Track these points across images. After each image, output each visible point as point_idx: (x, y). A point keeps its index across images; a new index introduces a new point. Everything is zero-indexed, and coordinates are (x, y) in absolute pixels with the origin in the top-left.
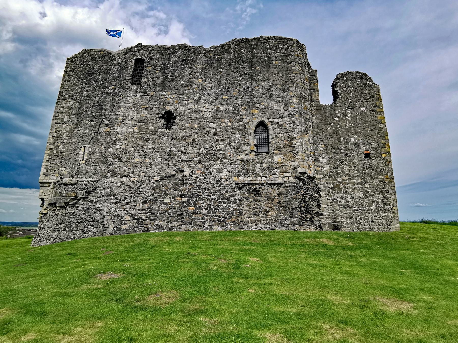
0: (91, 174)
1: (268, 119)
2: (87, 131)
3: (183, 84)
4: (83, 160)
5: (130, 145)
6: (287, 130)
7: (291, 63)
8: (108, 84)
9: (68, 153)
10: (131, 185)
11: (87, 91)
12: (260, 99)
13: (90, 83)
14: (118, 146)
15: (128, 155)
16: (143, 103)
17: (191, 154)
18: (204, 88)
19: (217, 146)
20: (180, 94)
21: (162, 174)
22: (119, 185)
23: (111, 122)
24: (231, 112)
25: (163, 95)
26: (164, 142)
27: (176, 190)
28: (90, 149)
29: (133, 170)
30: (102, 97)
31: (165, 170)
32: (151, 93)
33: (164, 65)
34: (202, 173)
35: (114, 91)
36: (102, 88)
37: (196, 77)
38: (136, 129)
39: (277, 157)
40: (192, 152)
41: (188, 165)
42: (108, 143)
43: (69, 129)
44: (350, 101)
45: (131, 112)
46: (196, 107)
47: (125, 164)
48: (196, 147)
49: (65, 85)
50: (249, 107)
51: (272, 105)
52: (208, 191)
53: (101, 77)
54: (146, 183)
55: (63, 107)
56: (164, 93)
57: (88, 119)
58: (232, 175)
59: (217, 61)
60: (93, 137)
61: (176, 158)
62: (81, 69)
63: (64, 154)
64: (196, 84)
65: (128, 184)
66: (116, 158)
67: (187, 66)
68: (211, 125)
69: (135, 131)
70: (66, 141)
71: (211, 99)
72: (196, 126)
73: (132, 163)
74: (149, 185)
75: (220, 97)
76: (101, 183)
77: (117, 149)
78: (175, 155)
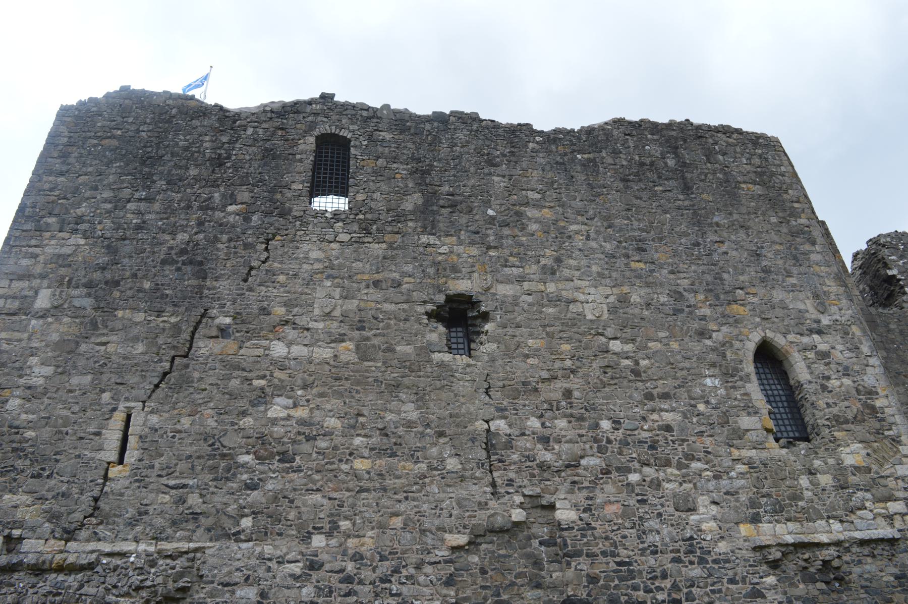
0: (159, 522)
1: (785, 335)
2: (140, 348)
3: (493, 218)
4: (121, 461)
5: (328, 407)
6: (846, 368)
7: (786, 192)
8: (223, 196)
9: (47, 433)
10: (350, 567)
11: (139, 213)
12: (741, 278)
13: (149, 188)
14: (277, 409)
15: (323, 444)
16: (360, 265)
17: (570, 441)
18: (563, 235)
19: (655, 416)
20: (489, 248)
21: (474, 521)
22: (296, 569)
23: (243, 322)
24: (667, 309)
25: (428, 245)
26: (462, 400)
27: (538, 586)
28: (154, 419)
29: (353, 506)
30: (201, 236)
31: (483, 505)
32: (388, 238)
33: (419, 160)
34: (627, 512)
35: (247, 219)
36: (200, 208)
37: (532, 203)
38: (347, 351)
39: (848, 450)
40: (571, 434)
41: (567, 485)
42: (233, 396)
43: (55, 337)
45: (320, 293)
46: (551, 287)
47: (314, 482)
48: (581, 419)
49: (47, 186)
50: (717, 297)
51: (778, 295)
52: (667, 584)
53: (193, 172)
54: (413, 558)
55: (35, 256)
56: (432, 240)
57: (143, 305)
58: (733, 515)
59: (584, 165)
60: (165, 374)
61: (515, 457)
62: (115, 143)
63: (30, 434)
64: (538, 221)
65: (337, 565)
66: (271, 456)
67: (498, 170)
68: (615, 346)
69: (343, 358)
70: (41, 381)
71: (595, 268)
72: (566, 347)
73: (342, 477)
74: (428, 569)
75: (620, 263)
76: (211, 561)
77: (274, 421)
78: (509, 445)
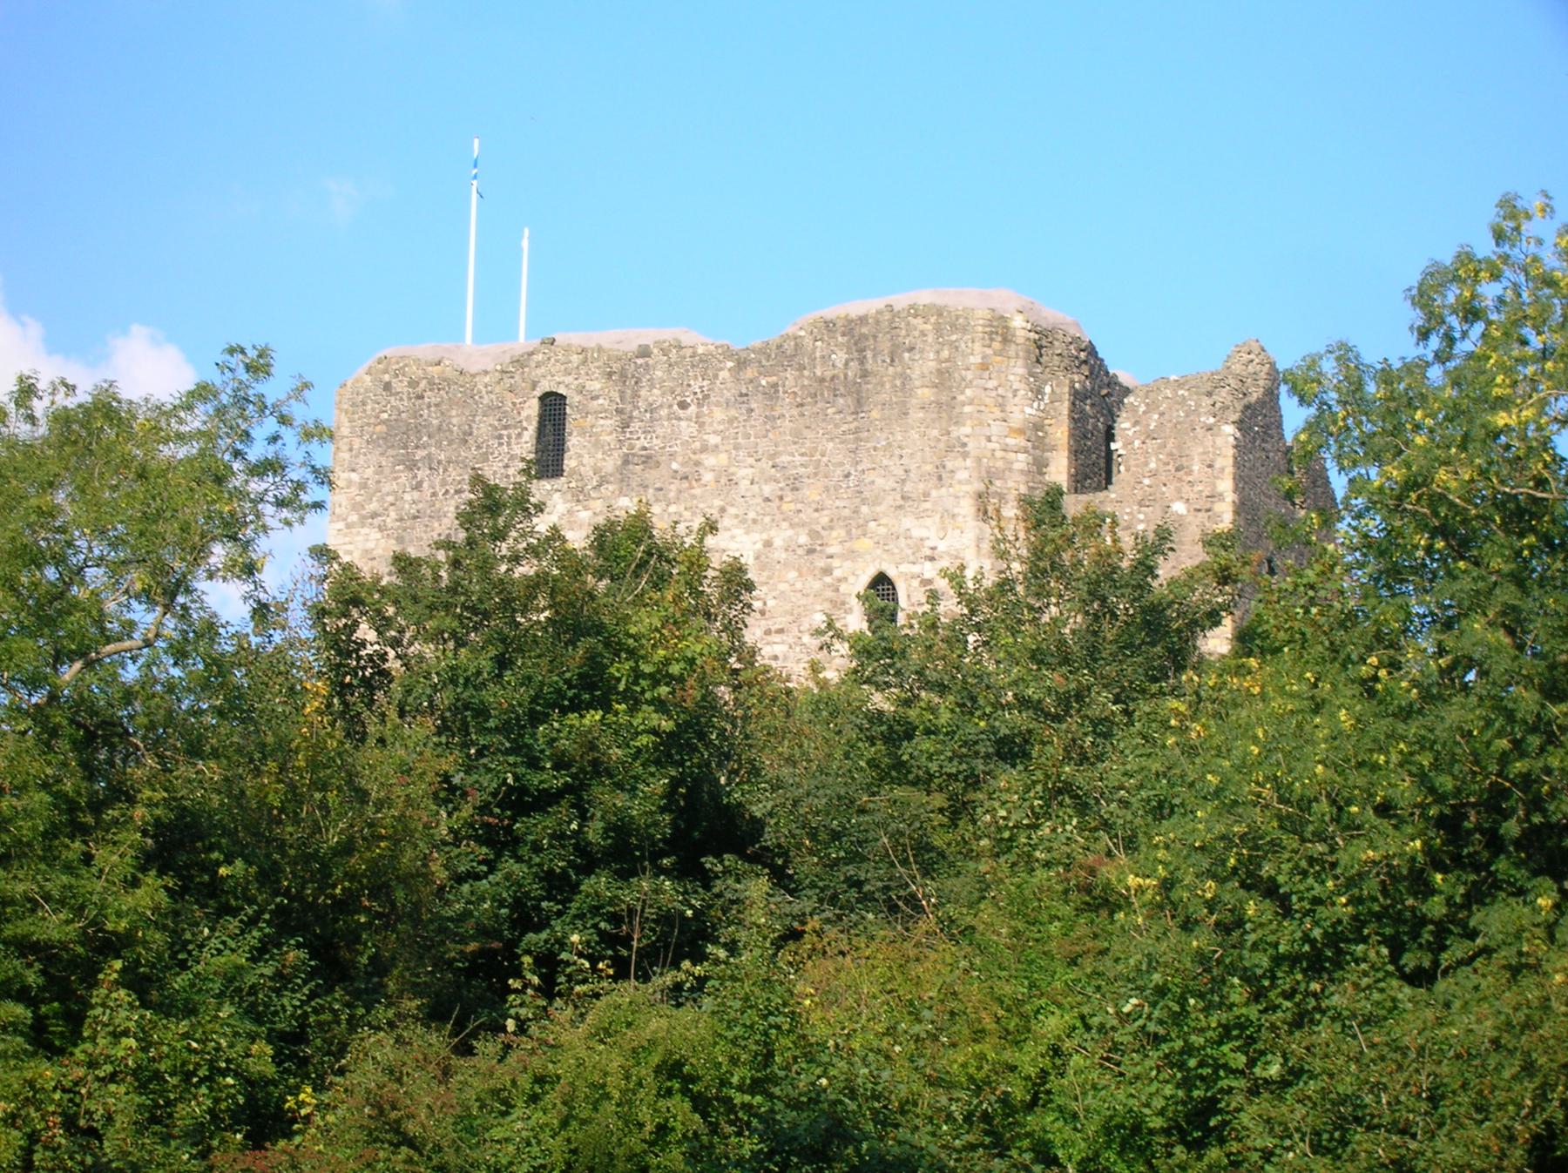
44: (1147, 481)
